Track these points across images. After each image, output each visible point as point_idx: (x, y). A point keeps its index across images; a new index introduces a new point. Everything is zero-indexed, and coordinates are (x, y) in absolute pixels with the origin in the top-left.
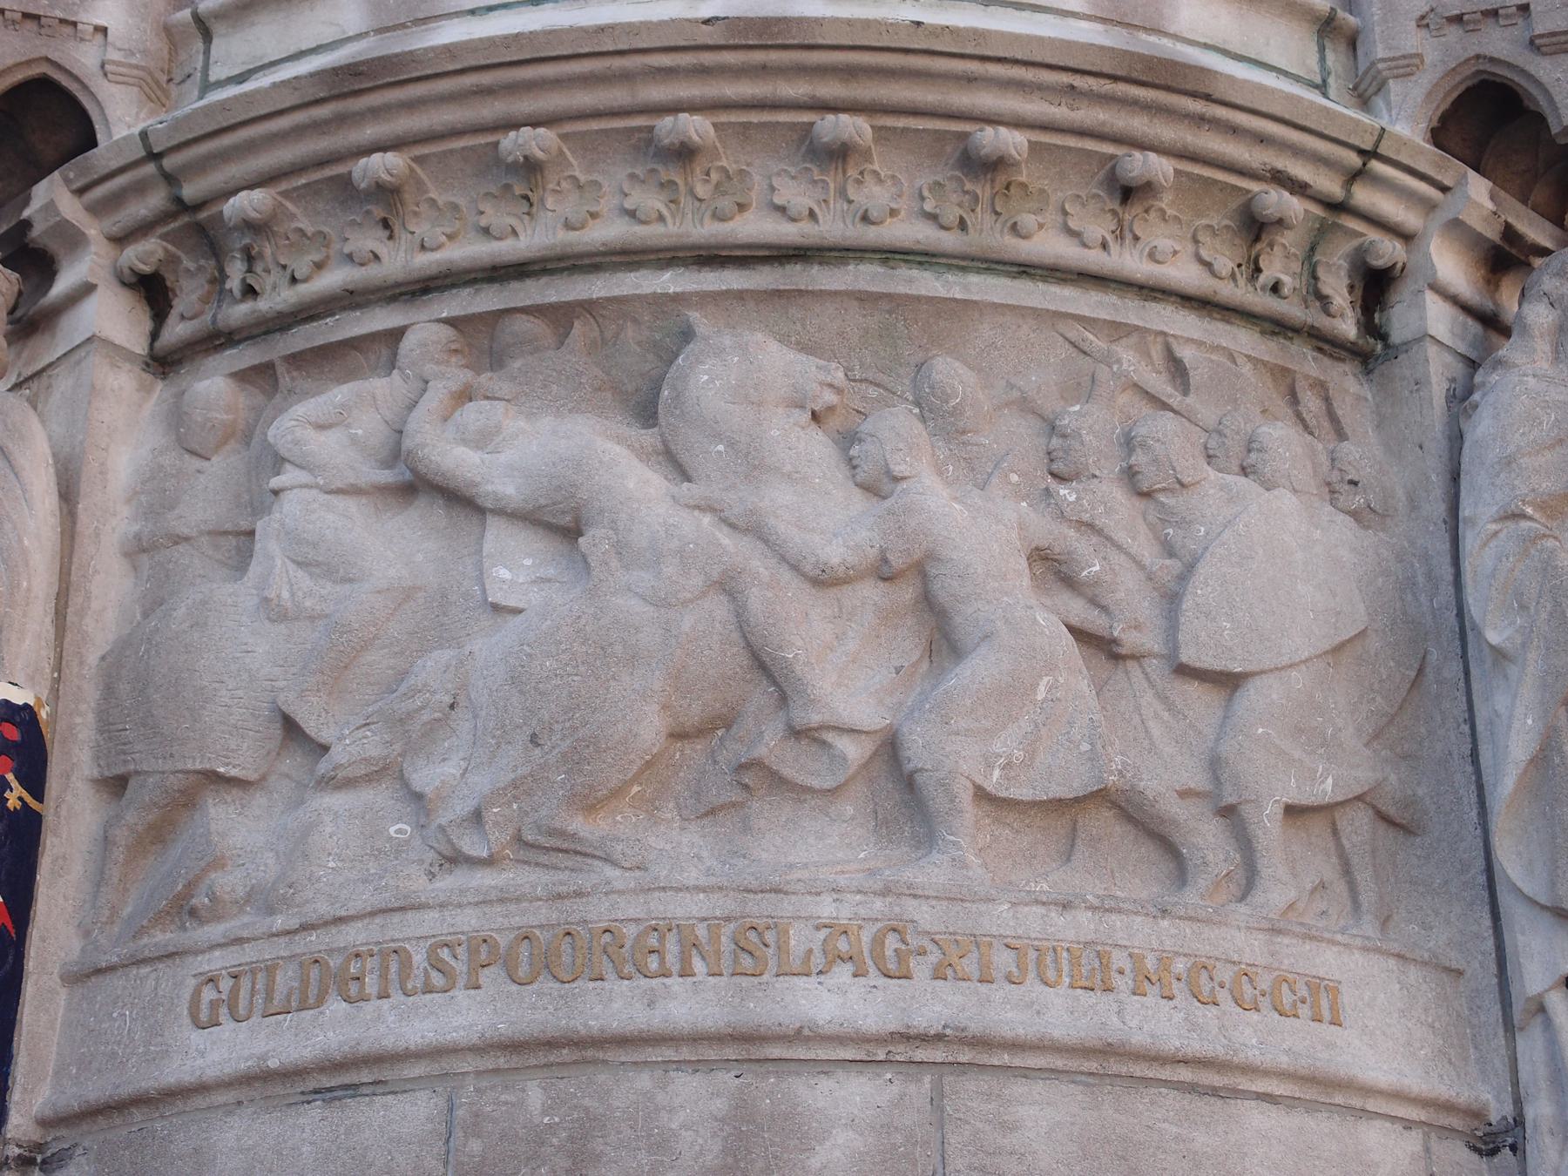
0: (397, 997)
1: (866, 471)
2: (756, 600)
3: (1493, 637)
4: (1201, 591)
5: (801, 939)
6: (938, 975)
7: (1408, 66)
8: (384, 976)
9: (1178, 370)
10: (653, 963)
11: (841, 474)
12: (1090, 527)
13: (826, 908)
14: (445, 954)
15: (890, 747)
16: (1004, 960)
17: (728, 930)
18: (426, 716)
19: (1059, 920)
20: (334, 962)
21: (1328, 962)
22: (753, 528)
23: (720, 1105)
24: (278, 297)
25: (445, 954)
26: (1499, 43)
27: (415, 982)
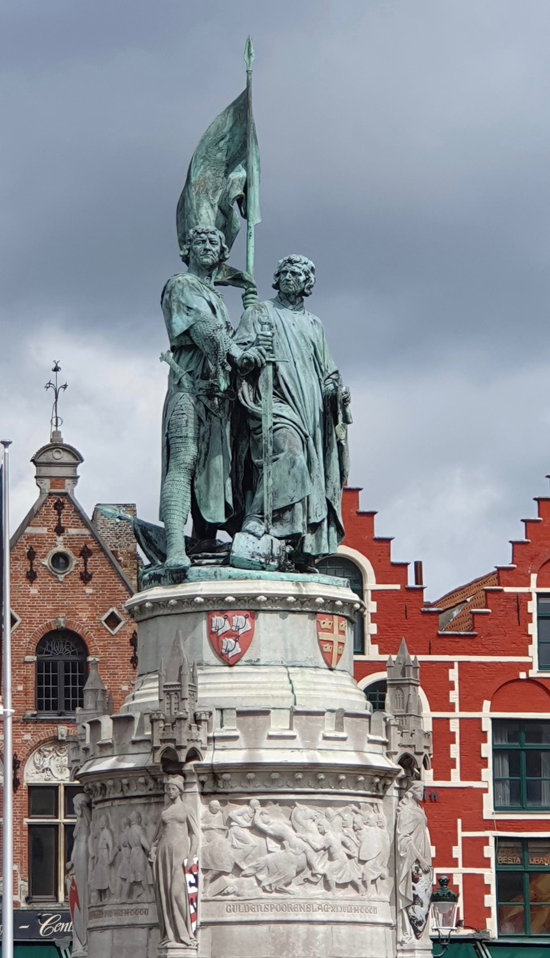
0: (260, 912)
1: (321, 831)
2: (309, 854)
3: (402, 855)
4: (363, 847)
5: (315, 906)
6: (332, 911)
7: (396, 753)
8: (258, 908)
9: (359, 807)
10: (296, 910)
11: (317, 830)
12: (348, 836)
13: (318, 902)
14: (267, 906)
15: (324, 876)
16: (339, 909)
17: (306, 905)
18: (260, 868)
19: (346, 902)
20: (250, 905)
21: (375, 904)
22: (307, 841)
23: (305, 930)
24: (230, 790)
25: (267, 906)
26: (410, 751)
27: (263, 910)
